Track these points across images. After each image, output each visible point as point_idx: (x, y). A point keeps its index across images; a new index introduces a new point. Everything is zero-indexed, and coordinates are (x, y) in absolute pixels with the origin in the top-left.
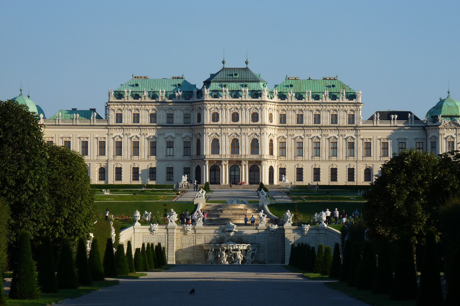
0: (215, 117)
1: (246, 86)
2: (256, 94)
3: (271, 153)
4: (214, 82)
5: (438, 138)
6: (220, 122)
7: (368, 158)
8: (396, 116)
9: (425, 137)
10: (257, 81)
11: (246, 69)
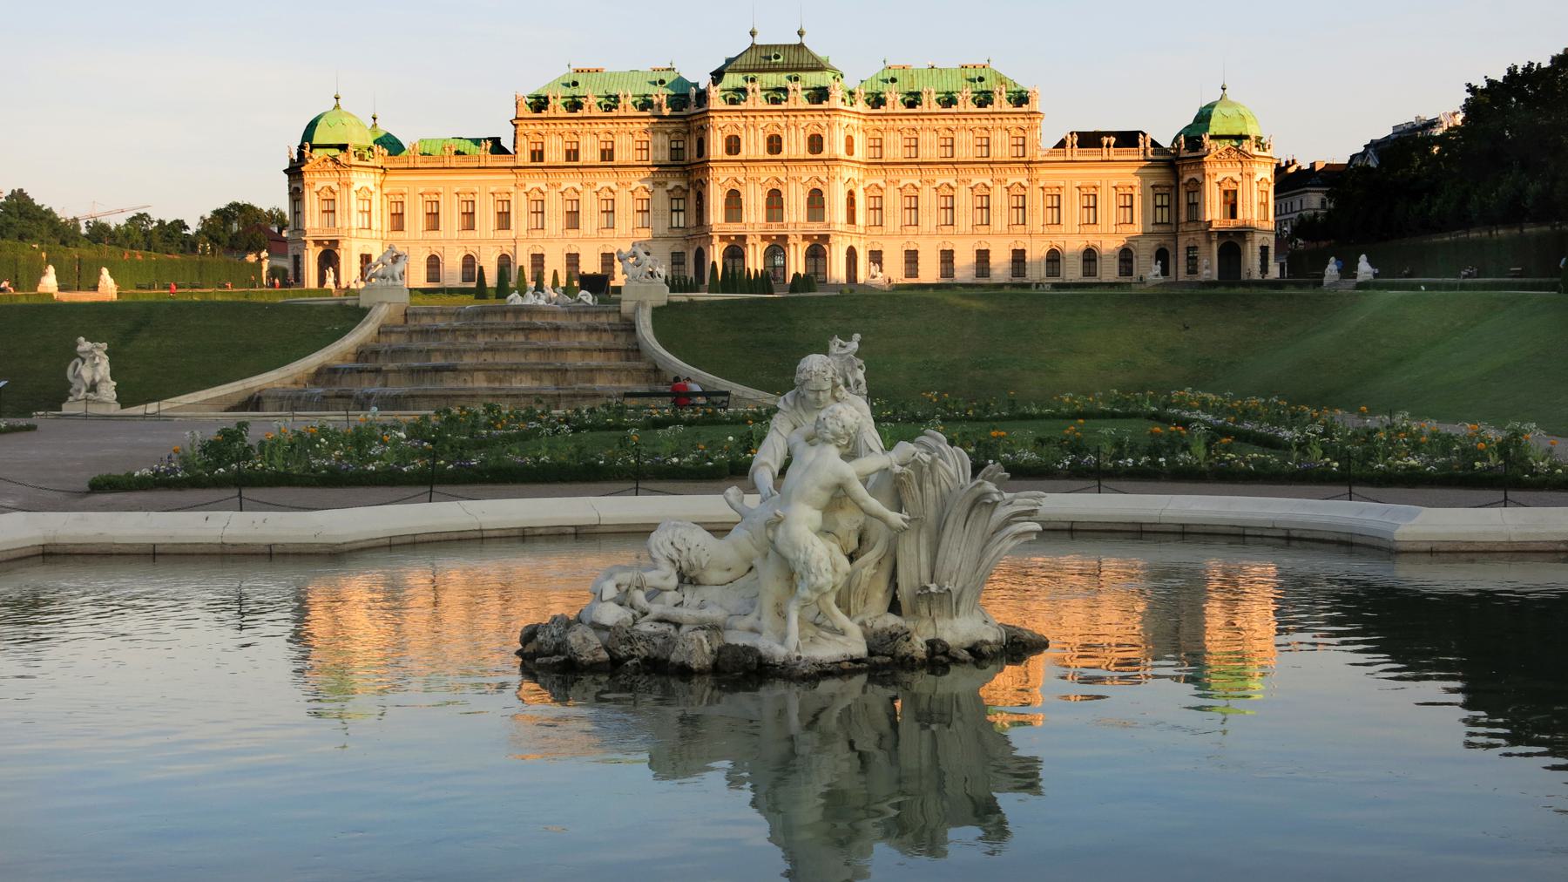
0: (733, 145)
1: (796, 79)
2: (820, 95)
3: (851, 218)
4: (732, 71)
5: (1203, 183)
6: (741, 156)
7: (1056, 229)
8: (1113, 140)
9: (1173, 183)
10: (819, 67)
11: (801, 46)
